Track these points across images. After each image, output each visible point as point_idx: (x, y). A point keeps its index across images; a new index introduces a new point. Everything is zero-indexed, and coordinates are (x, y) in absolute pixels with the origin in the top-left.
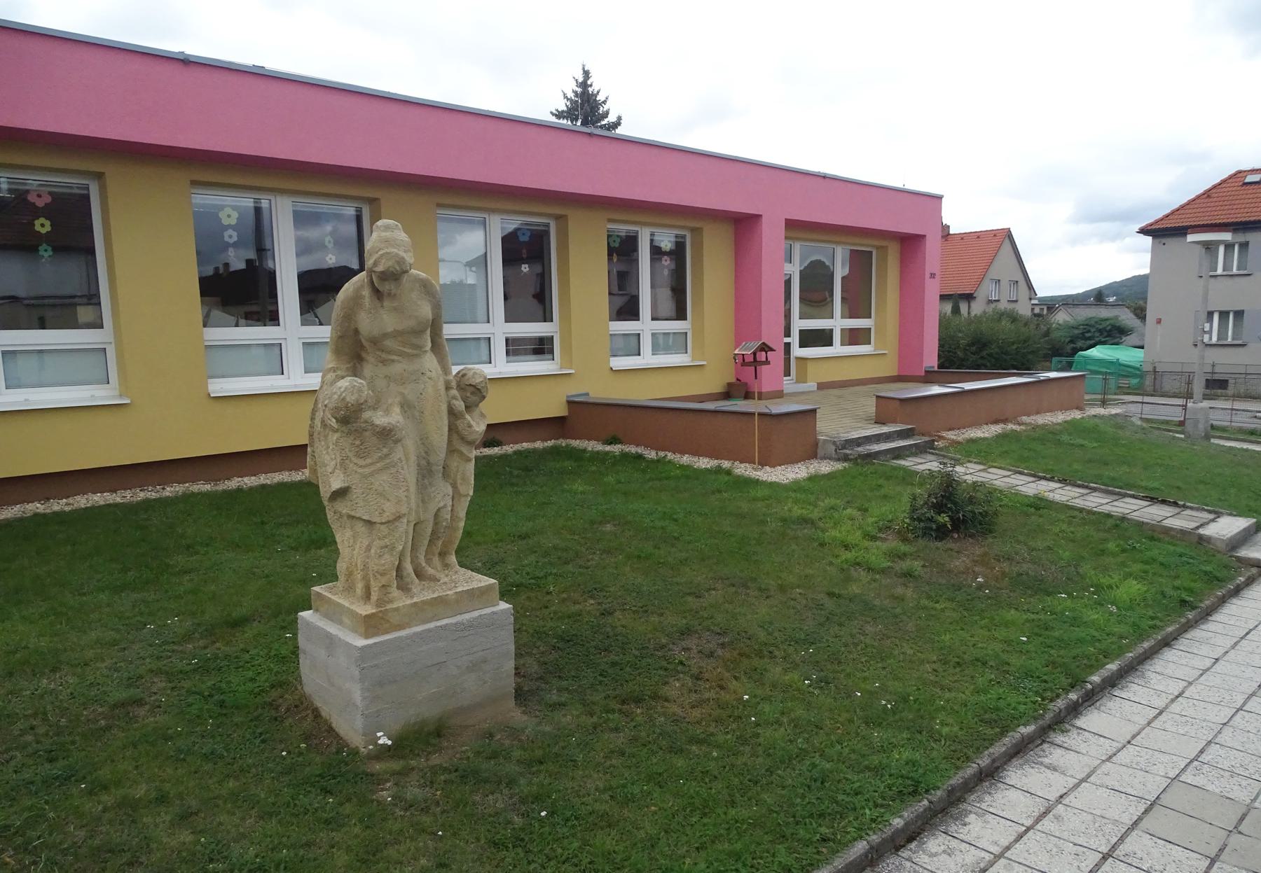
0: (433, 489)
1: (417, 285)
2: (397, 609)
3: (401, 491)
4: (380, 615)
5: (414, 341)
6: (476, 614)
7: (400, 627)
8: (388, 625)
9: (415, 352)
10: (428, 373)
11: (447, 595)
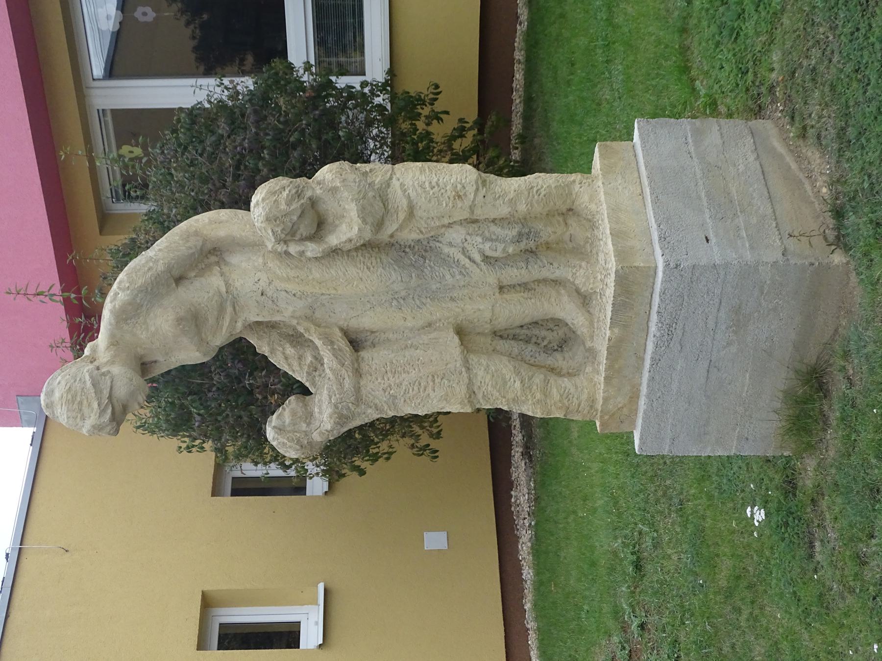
0: (448, 277)
1: (126, 327)
2: (606, 400)
3: (432, 394)
4: (606, 417)
5: (211, 320)
6: (654, 317)
7: (634, 397)
8: (625, 411)
9: (229, 309)
10: (263, 284)
11: (609, 340)
